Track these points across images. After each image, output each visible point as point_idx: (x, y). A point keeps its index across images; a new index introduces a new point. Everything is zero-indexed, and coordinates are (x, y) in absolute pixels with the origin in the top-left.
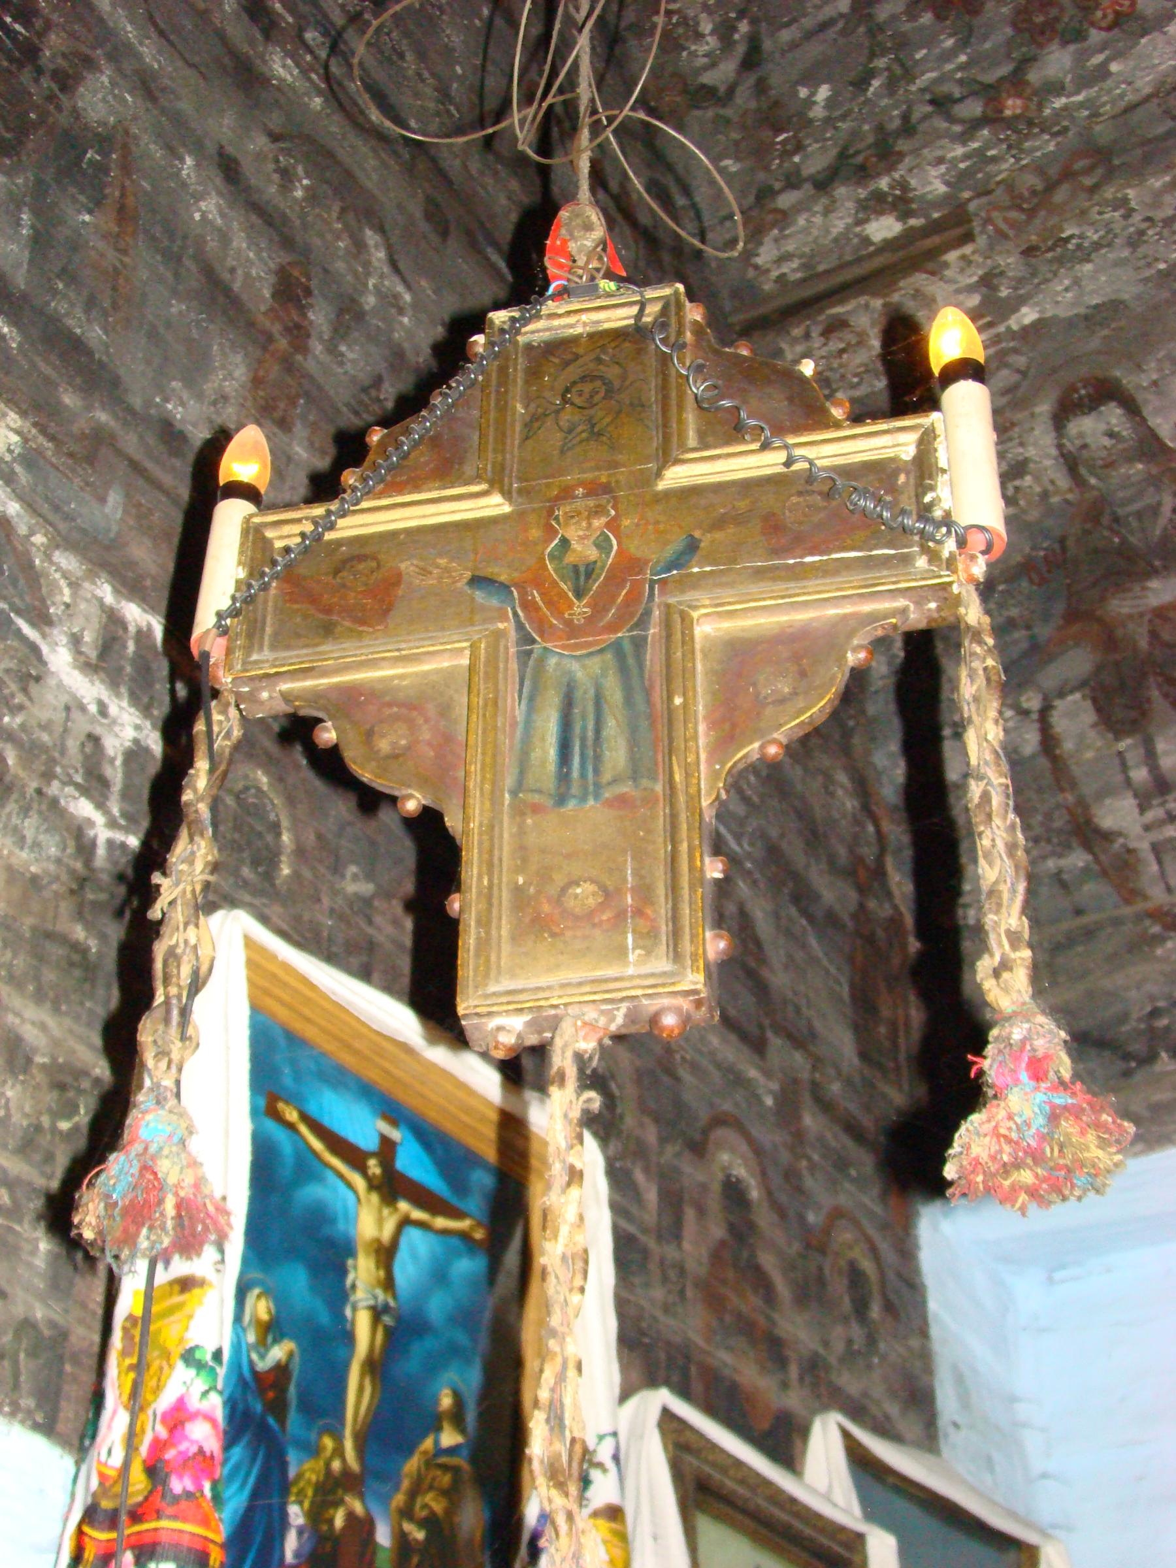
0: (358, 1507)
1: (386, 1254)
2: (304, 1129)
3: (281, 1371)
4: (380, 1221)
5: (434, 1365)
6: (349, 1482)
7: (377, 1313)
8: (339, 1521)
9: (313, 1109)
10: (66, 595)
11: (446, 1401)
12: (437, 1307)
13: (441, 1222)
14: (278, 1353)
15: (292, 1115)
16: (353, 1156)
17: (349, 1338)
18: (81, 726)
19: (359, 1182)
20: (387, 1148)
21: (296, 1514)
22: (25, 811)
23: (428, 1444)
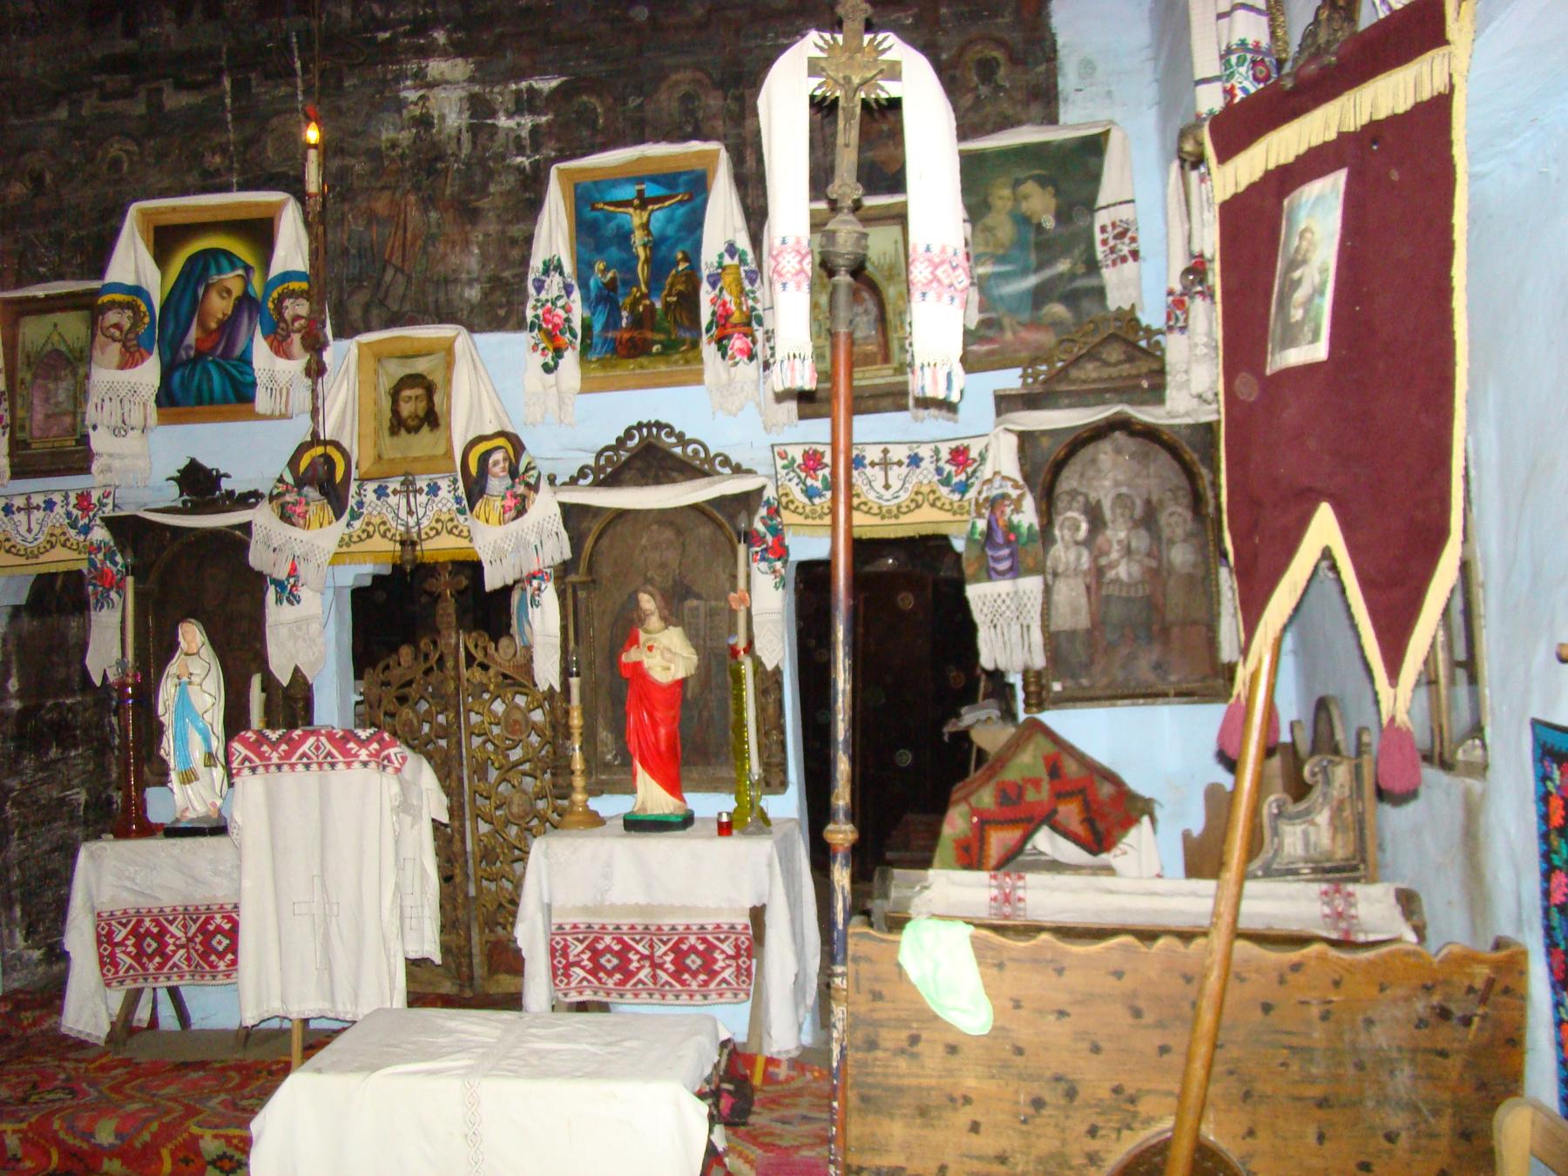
0: (647, 302)
1: (646, 226)
2: (606, 207)
3: (613, 280)
4: (641, 217)
5: (672, 249)
6: (644, 296)
7: (645, 246)
8: (641, 309)
9: (608, 198)
10: (500, 99)
11: (680, 256)
12: (670, 231)
13: (667, 204)
14: (610, 275)
15: (600, 206)
16: (627, 204)
17: (637, 257)
18: (512, 135)
19: (631, 210)
20: (640, 193)
21: (625, 314)
22: (500, 175)
23: (674, 272)
